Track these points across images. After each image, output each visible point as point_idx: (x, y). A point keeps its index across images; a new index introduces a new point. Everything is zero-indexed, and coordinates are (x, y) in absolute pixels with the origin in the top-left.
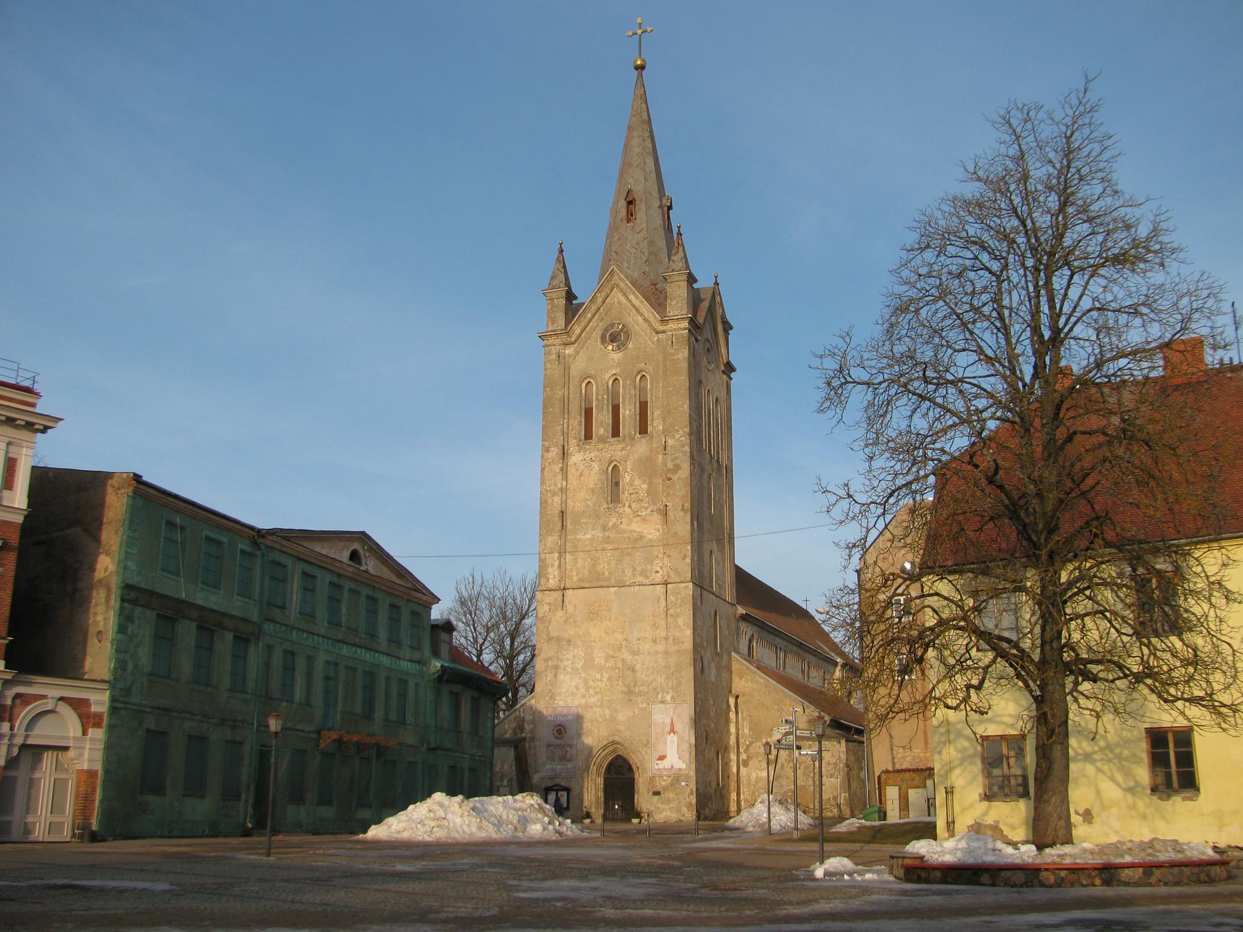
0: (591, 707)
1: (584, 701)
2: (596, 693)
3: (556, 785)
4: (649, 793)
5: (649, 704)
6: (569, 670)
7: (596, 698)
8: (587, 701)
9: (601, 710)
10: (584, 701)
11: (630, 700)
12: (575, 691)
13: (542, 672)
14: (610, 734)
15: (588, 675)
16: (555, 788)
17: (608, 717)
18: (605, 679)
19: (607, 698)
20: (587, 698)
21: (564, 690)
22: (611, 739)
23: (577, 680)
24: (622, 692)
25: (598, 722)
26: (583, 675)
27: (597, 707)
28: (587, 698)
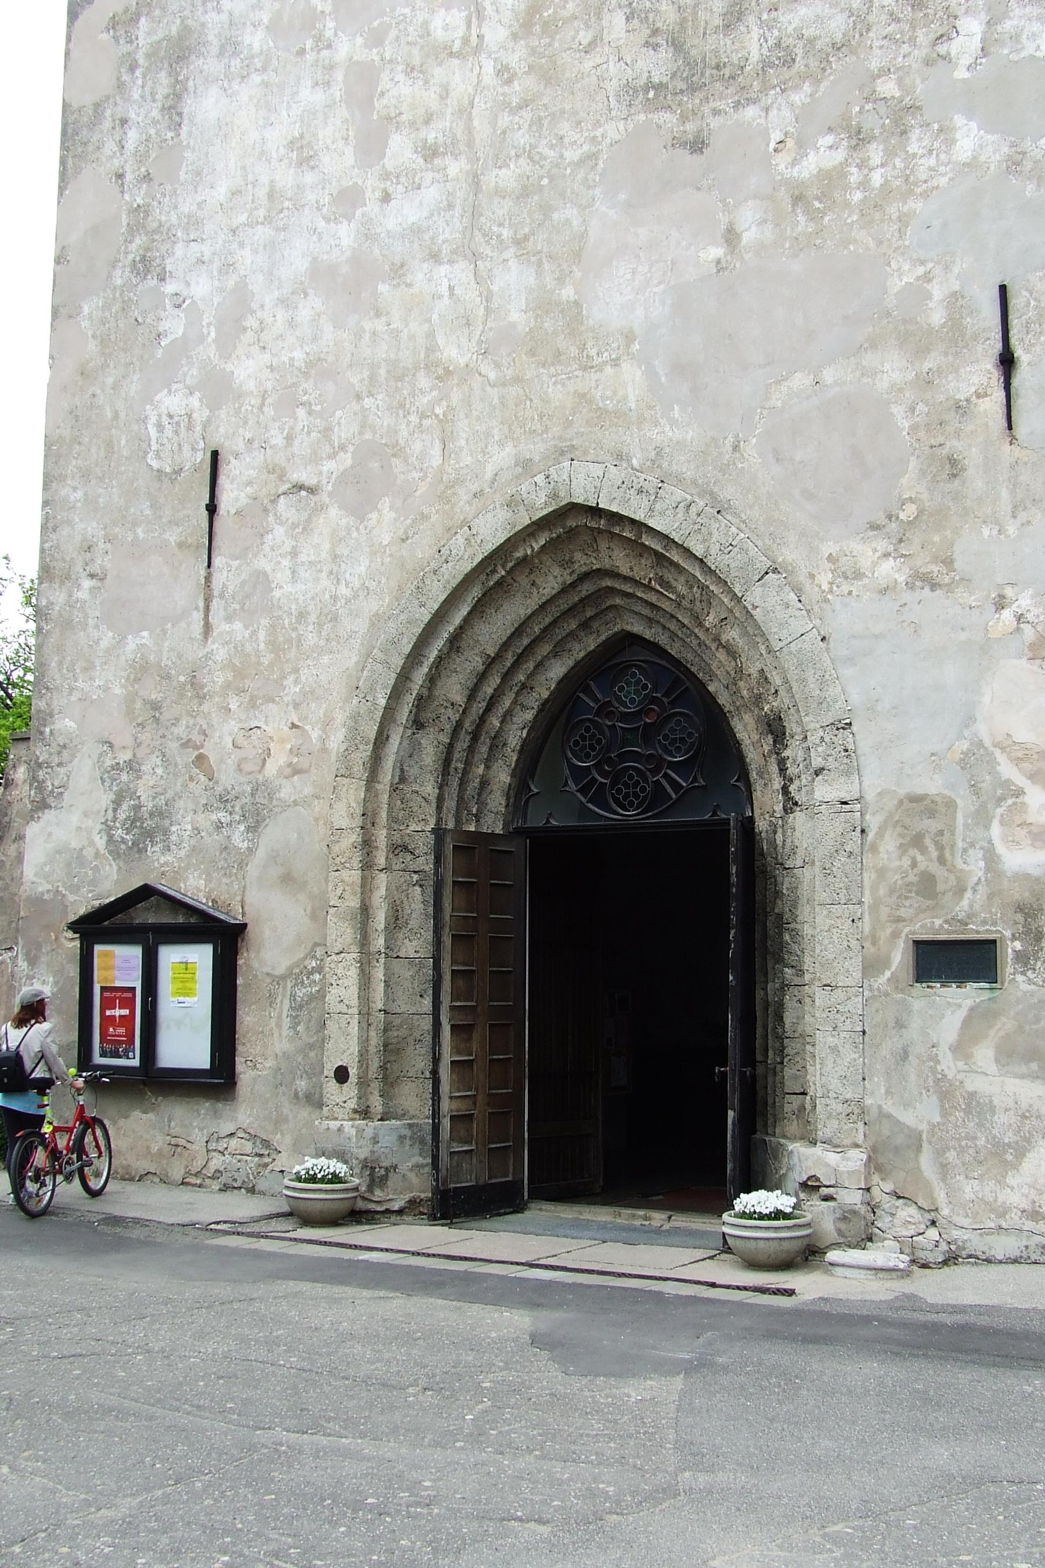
0: (398, 272)
1: (346, 234)
2: (430, 153)
3: (145, 892)
4: (871, 967)
5: (859, 139)
6: (255, 40)
7: (431, 194)
8: (368, 235)
9: (461, 272)
10: (346, 234)
11: (698, 145)
12: (286, 178)
13: (98, 107)
14: (536, 449)
15: (376, 39)
16: (146, 915)
17: (517, 316)
18: (495, 34)
19: (507, 177)
20: (372, 207)
21: (221, 192)
22: (541, 505)
23: (310, 96)
24: (630, 91)
25: (444, 374)
26: (345, 48)
27: (435, 257)
28: (372, 207)
